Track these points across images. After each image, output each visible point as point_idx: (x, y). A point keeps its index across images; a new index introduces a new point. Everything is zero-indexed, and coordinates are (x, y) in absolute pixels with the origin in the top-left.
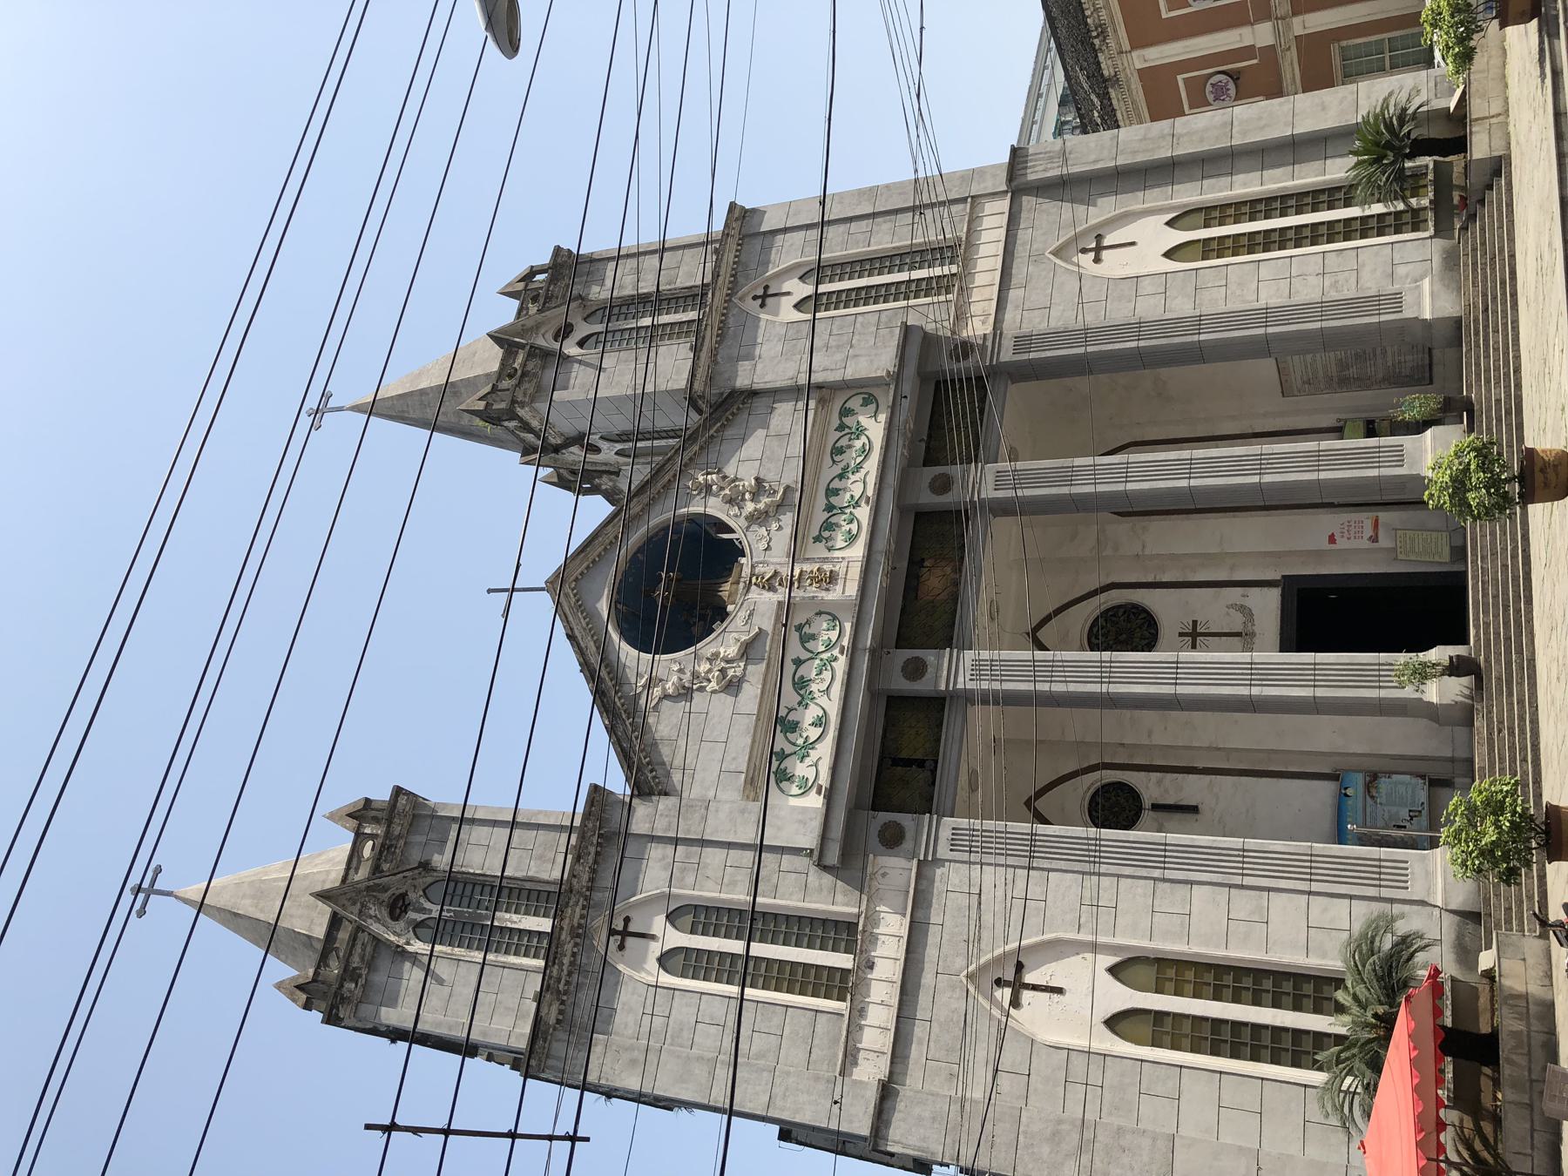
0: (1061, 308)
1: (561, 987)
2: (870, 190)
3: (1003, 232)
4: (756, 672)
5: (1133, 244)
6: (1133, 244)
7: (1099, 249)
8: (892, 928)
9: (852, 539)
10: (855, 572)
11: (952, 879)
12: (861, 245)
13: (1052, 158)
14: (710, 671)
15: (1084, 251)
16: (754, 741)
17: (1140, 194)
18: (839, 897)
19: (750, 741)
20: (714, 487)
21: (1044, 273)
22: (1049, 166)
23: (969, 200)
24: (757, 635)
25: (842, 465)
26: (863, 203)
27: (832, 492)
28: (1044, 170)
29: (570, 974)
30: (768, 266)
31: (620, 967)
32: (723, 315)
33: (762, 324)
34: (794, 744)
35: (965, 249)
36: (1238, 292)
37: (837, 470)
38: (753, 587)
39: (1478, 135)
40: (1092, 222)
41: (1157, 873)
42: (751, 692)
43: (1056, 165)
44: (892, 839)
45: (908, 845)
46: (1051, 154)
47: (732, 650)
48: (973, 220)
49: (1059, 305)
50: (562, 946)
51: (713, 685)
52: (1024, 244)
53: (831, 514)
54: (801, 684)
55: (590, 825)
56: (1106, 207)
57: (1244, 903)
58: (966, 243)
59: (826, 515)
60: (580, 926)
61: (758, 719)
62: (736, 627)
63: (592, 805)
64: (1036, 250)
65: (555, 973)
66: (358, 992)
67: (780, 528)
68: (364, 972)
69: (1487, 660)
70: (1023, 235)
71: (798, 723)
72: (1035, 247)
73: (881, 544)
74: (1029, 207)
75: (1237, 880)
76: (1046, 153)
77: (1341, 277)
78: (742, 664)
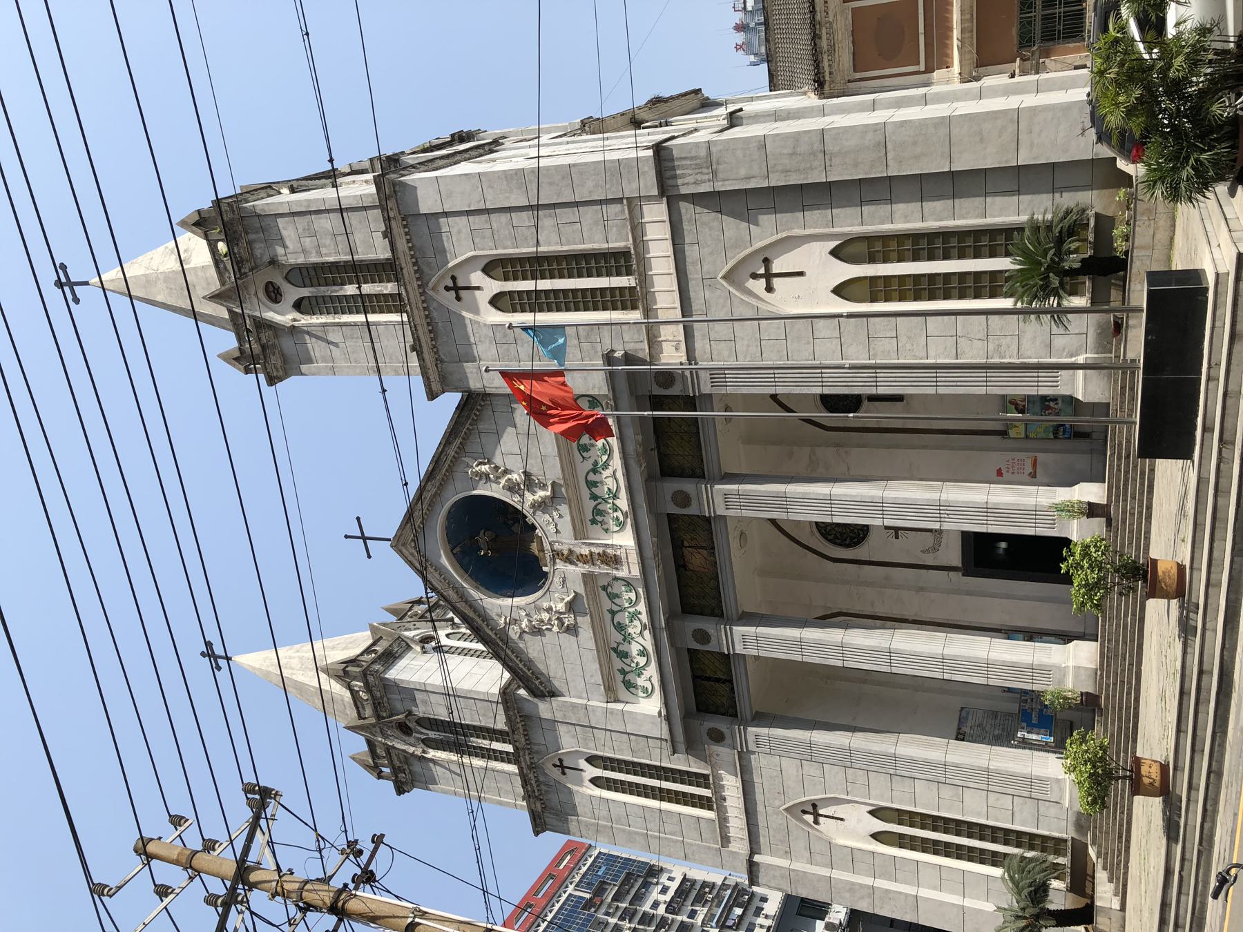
0: (745, 342)
1: (537, 794)
2: (516, 174)
3: (669, 244)
4: (584, 622)
5: (801, 274)
6: (801, 274)
7: (769, 276)
8: (731, 786)
9: (622, 525)
10: (634, 557)
11: (762, 764)
12: (531, 244)
13: (699, 166)
14: (550, 619)
15: (755, 276)
16: (601, 665)
17: (800, 215)
18: (692, 764)
19: (598, 666)
20: (491, 476)
21: (721, 301)
22: (699, 177)
23: (625, 201)
24: (574, 597)
25: (591, 461)
26: (515, 190)
27: (591, 484)
28: (695, 183)
29: (538, 786)
30: (446, 256)
31: (569, 785)
32: (425, 309)
33: (468, 322)
34: (630, 666)
35: (637, 262)
36: (908, 346)
37: (588, 465)
38: (558, 561)
39: (1134, 330)
40: (758, 245)
41: (892, 772)
42: (586, 633)
43: (706, 177)
44: (718, 737)
45: (728, 741)
46: (698, 161)
47: (561, 606)
48: (637, 229)
49: (743, 339)
50: (527, 776)
51: (555, 629)
52: (694, 263)
53: (596, 502)
54: (620, 627)
55: (512, 713)
56: (767, 230)
57: (946, 792)
58: (636, 256)
59: (593, 503)
60: (532, 763)
61: (598, 651)
62: (556, 588)
63: (507, 703)
64: (709, 273)
65: (529, 789)
66: (409, 776)
67: (561, 516)
68: (406, 767)
69: (1106, 706)
70: (691, 252)
71: (627, 653)
72: (705, 268)
73: (649, 553)
74: (689, 216)
75: (943, 780)
76: (692, 158)
77: (1004, 341)
78: (572, 616)
